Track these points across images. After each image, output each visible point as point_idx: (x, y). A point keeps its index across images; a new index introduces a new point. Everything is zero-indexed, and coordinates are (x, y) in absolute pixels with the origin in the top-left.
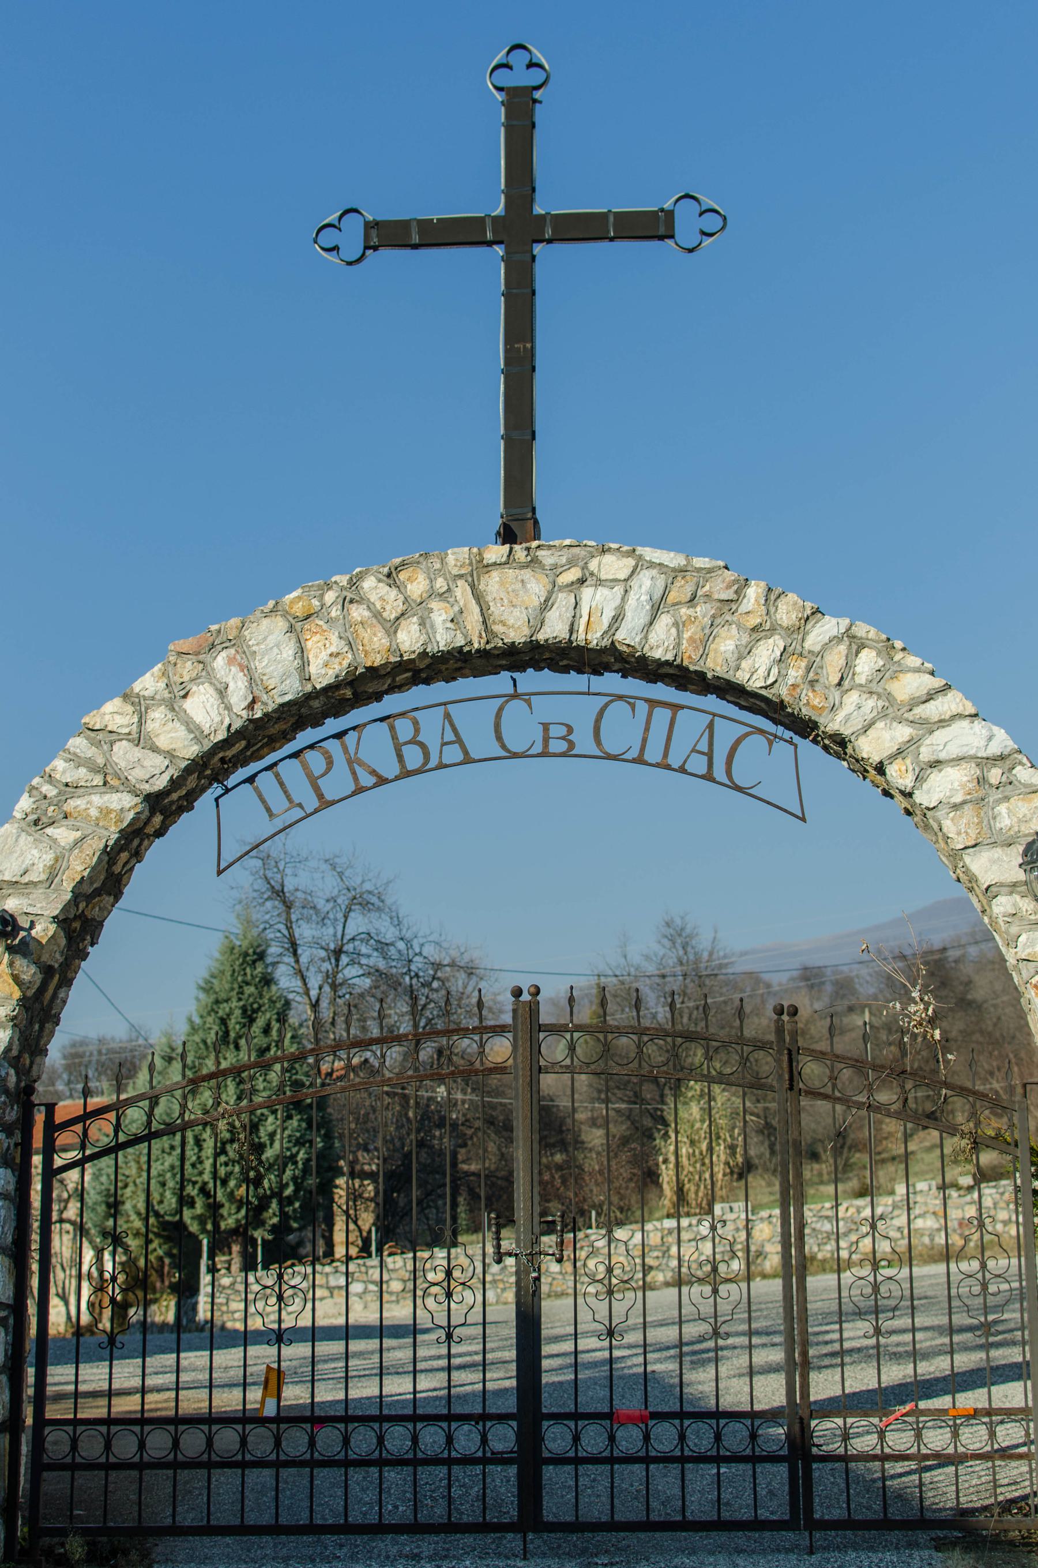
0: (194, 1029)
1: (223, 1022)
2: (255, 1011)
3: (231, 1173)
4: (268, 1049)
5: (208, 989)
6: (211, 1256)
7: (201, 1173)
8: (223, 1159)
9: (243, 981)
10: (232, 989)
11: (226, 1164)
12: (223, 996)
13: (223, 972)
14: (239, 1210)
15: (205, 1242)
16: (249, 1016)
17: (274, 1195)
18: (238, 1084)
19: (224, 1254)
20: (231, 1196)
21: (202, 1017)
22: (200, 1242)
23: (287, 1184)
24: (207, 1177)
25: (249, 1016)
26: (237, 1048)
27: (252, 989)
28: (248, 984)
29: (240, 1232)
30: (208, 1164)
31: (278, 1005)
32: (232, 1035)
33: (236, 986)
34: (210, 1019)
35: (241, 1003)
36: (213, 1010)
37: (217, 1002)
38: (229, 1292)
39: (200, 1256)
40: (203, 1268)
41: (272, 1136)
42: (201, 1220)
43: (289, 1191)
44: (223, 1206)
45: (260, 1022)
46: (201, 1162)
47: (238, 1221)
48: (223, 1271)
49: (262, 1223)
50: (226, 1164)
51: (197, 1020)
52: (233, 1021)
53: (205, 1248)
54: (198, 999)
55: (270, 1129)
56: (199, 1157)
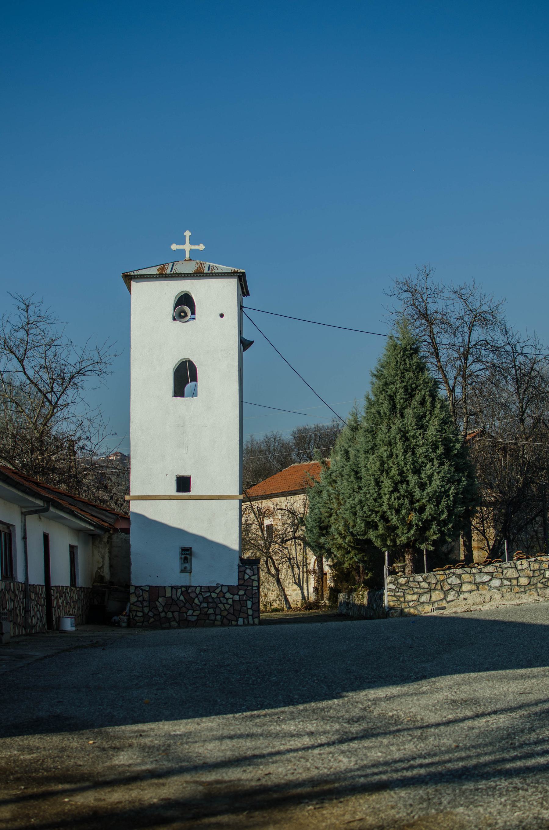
0: (371, 404)
1: (391, 398)
2: (413, 390)
3: (403, 504)
4: (424, 416)
5: (379, 375)
6: (390, 564)
7: (381, 505)
8: (396, 494)
9: (404, 369)
10: (397, 375)
11: (399, 499)
12: (390, 379)
13: (389, 363)
14: (409, 530)
15: (386, 553)
16: (410, 393)
17: (434, 519)
18: (404, 442)
19: (400, 562)
20: (403, 521)
21: (376, 395)
22: (384, 553)
23: (443, 512)
24: (385, 508)
25: (410, 393)
26: (402, 416)
27: (411, 374)
28: (407, 371)
29: (410, 546)
30: (385, 498)
31: (430, 385)
32: (398, 407)
33: (399, 372)
34: (382, 397)
35: (404, 384)
36: (384, 390)
37: (386, 384)
38: (405, 588)
39: (384, 564)
40: (386, 572)
41: (430, 477)
42: (383, 538)
43: (444, 516)
44: (398, 528)
45: (418, 397)
46: (381, 498)
47: (408, 538)
48: (400, 574)
49: (427, 539)
50: (399, 499)
51: (373, 398)
52: (398, 397)
53: (387, 558)
54: (372, 383)
55: (429, 472)
56: (379, 494)
